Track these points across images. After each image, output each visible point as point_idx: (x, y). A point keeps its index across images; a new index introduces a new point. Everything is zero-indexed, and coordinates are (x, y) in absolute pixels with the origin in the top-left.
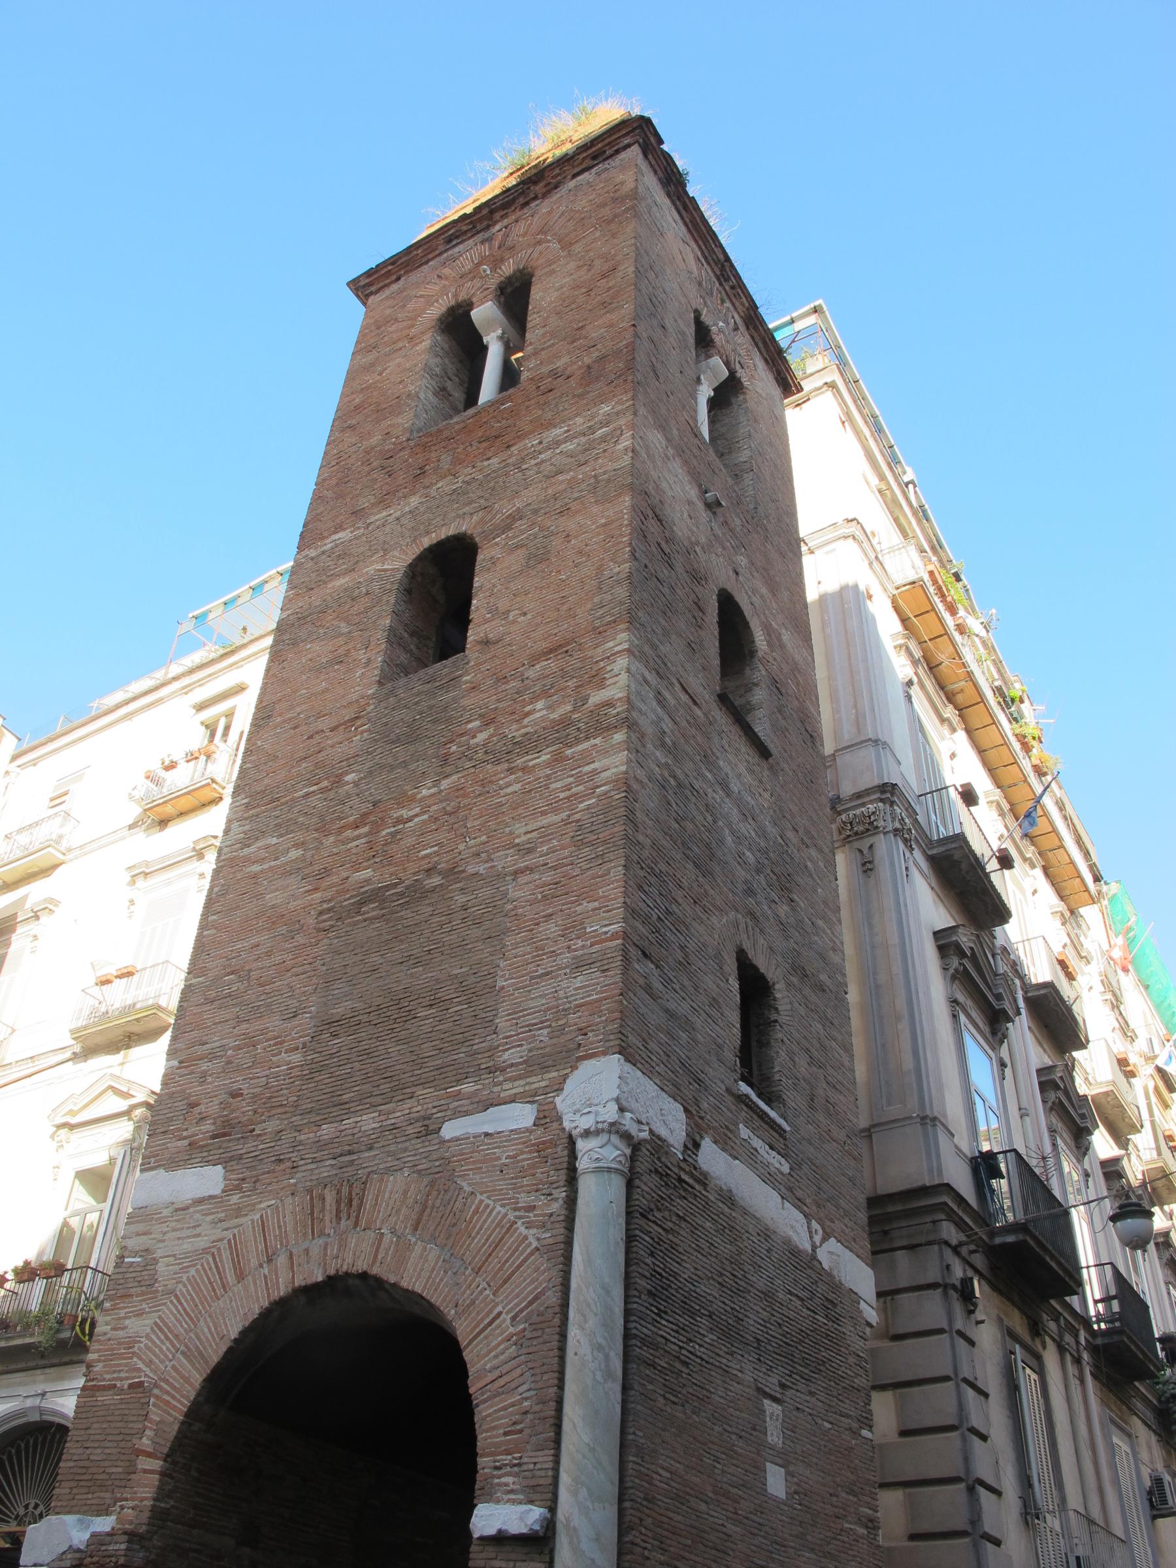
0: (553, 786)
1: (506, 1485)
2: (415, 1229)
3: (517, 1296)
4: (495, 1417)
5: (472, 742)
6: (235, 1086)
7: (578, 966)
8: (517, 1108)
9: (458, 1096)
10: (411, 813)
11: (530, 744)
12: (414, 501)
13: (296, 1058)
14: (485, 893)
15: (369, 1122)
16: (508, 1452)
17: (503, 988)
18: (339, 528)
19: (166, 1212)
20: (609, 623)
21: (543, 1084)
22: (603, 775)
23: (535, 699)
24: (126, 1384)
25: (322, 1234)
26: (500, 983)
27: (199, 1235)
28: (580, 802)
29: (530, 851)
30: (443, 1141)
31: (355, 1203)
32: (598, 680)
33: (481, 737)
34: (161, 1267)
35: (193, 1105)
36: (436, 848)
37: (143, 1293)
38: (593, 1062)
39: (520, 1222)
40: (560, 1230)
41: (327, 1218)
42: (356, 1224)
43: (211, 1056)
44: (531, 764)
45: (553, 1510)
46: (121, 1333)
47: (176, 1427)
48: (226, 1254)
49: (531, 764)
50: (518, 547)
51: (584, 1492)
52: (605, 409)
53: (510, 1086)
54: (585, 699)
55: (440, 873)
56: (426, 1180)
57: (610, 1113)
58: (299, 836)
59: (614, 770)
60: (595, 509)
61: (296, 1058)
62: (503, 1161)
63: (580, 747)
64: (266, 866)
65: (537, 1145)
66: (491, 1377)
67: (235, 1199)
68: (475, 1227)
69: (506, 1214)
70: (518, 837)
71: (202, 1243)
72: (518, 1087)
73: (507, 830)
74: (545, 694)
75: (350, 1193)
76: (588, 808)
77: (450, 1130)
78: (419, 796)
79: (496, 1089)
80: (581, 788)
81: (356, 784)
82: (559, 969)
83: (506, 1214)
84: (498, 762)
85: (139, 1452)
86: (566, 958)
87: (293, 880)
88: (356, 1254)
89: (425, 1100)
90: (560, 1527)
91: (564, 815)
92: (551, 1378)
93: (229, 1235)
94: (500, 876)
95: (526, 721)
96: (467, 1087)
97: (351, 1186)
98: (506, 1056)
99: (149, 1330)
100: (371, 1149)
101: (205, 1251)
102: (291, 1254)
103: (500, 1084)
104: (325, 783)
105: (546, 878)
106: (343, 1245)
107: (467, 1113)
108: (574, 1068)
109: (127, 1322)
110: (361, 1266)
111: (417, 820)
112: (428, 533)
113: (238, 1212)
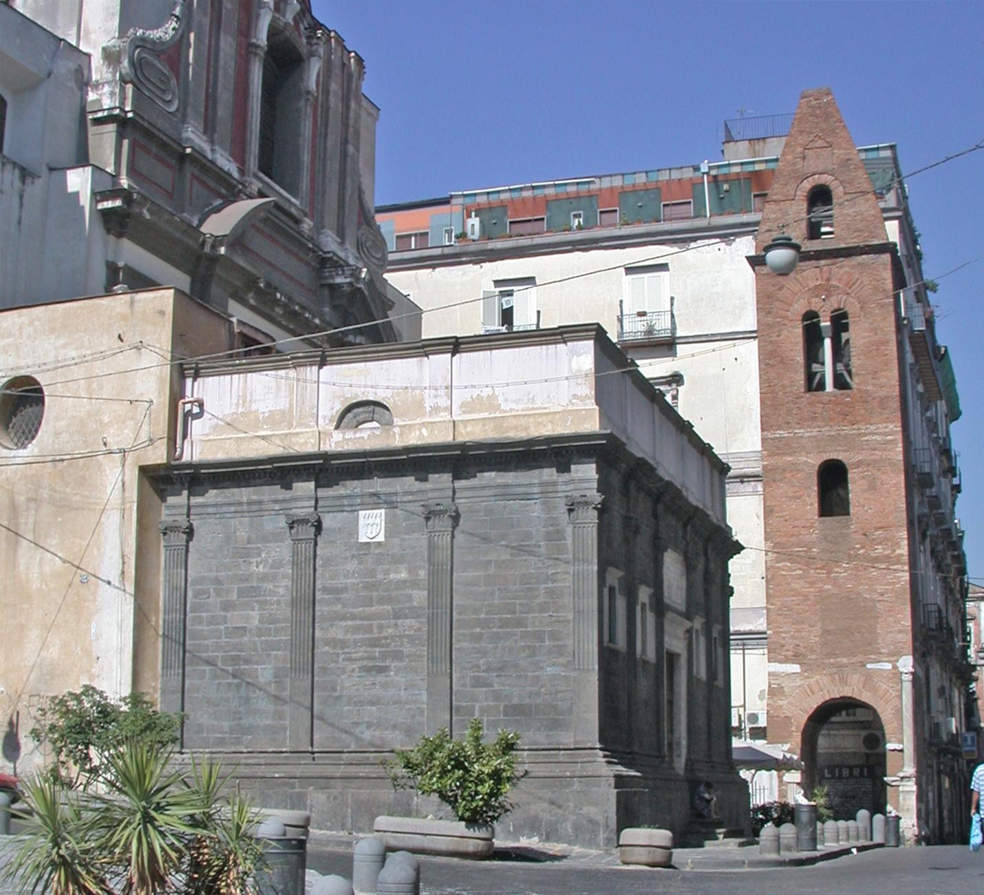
4: (888, 729)
7: (900, 632)
11: (876, 559)
13: (817, 639)
14: (870, 604)
15: (845, 660)
32: (898, 545)
33: (861, 551)
35: (783, 646)
43: (785, 633)
50: (863, 478)
58: (799, 566)
60: (891, 475)
61: (817, 639)
71: (798, 684)
77: (869, 666)
89: (860, 658)
94: (874, 601)
96: (872, 656)
110: (849, 695)
113: (808, 678)
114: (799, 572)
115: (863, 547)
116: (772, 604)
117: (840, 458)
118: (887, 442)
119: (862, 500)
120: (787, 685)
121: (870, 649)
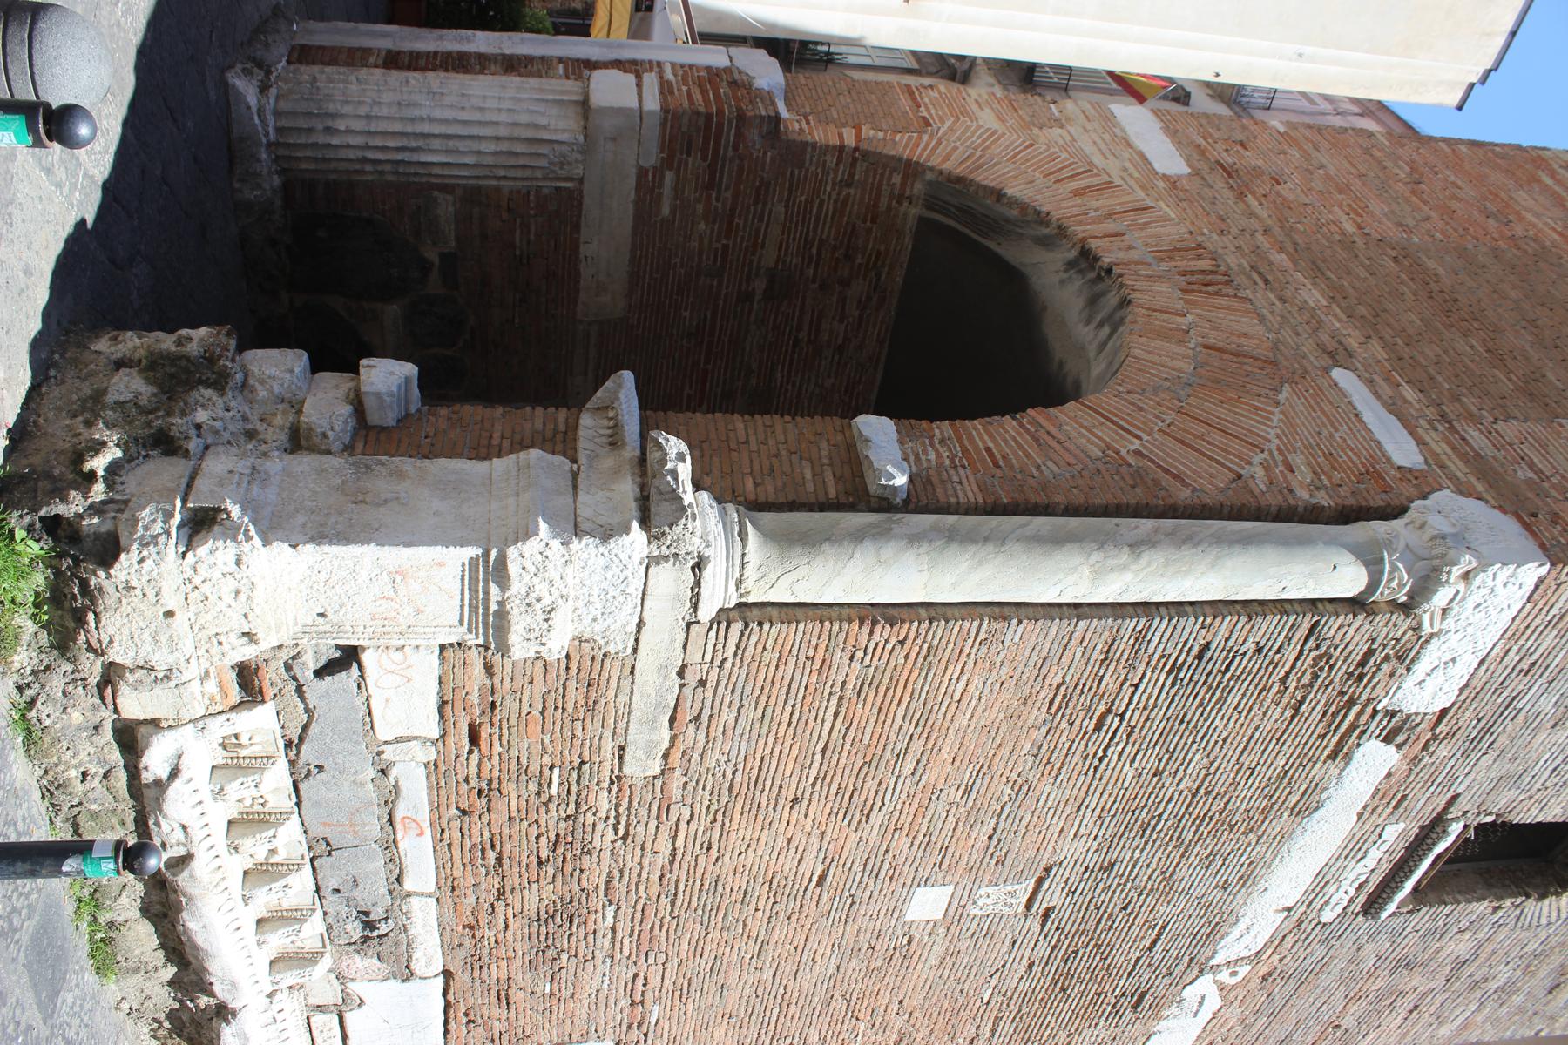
1: (925, 452)
4: (1002, 437)
8: (1411, 445)
16: (965, 451)
19: (1117, 131)
24: (925, 114)
31: (1210, 288)
39: (1265, 455)
40: (1273, 501)
46: (975, 107)
47: (893, 153)
64: (1557, 188)
65: (1376, 471)
72: (1440, 447)
92: (1078, 498)
93: (1118, 181)
96: (1409, 393)
101: (1091, 163)
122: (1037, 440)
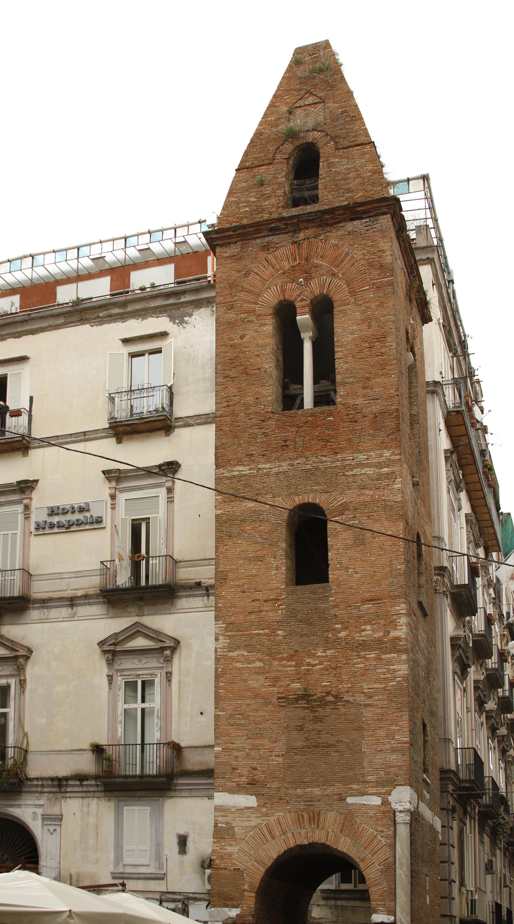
0: (378, 671)
2: (341, 832)
3: (380, 858)
5: (339, 635)
6: (254, 765)
7: (394, 750)
9: (351, 788)
10: (315, 662)
11: (364, 646)
12: (285, 466)
13: (280, 760)
15: (317, 791)
17: (365, 752)
18: (240, 462)
19: (233, 810)
20: (397, 596)
21: (384, 791)
22: (399, 673)
23: (365, 624)
25: (305, 828)
26: (363, 750)
27: (251, 821)
28: (390, 682)
29: (371, 697)
30: (347, 804)
33: (343, 634)
34: (236, 829)
35: (234, 769)
36: (329, 683)
37: (230, 838)
38: (401, 787)
39: (378, 836)
41: (306, 823)
42: (318, 828)
43: (238, 750)
44: (367, 656)
45: (395, 917)
47: (258, 884)
48: (265, 830)
49: (367, 656)
51: (404, 913)
52: (387, 454)
53: (371, 789)
54: (388, 632)
55: (332, 696)
56: (343, 816)
57: (408, 806)
58: (260, 655)
59: (403, 672)
62: (371, 814)
63: (388, 656)
64: (245, 666)
65: (383, 811)
66: (373, 880)
67: (264, 810)
68: (363, 834)
69: (373, 832)
70: (365, 689)
71: (253, 823)
72: (374, 790)
73: (360, 685)
74: (369, 622)
75: (314, 816)
76: (393, 686)
77: (350, 800)
78: (317, 655)
79: (366, 789)
80: (389, 675)
81: (284, 637)
82: (387, 750)
83: (373, 832)
84: (352, 650)
85: (244, 890)
86: (388, 746)
87: (261, 678)
88: (318, 836)
89: (338, 788)
90: (397, 921)
91: (383, 686)
92: (393, 883)
95: (363, 634)
96: (355, 786)
97: (313, 813)
98: (369, 778)
99: (237, 851)
100: (319, 801)
101: (255, 827)
102: (293, 833)
103: (367, 788)
104: (267, 631)
105: (379, 711)
106: (314, 833)
107: (356, 796)
108: (394, 788)
109: (226, 847)
110: (323, 841)
111: (318, 666)
112: (297, 494)
113: (267, 815)
114: (258, 664)
115: (345, 628)
116: (223, 710)
117: (317, 501)
118: (380, 477)
119: (345, 561)
120: (239, 825)
121: (353, 776)
122: (376, 885)
